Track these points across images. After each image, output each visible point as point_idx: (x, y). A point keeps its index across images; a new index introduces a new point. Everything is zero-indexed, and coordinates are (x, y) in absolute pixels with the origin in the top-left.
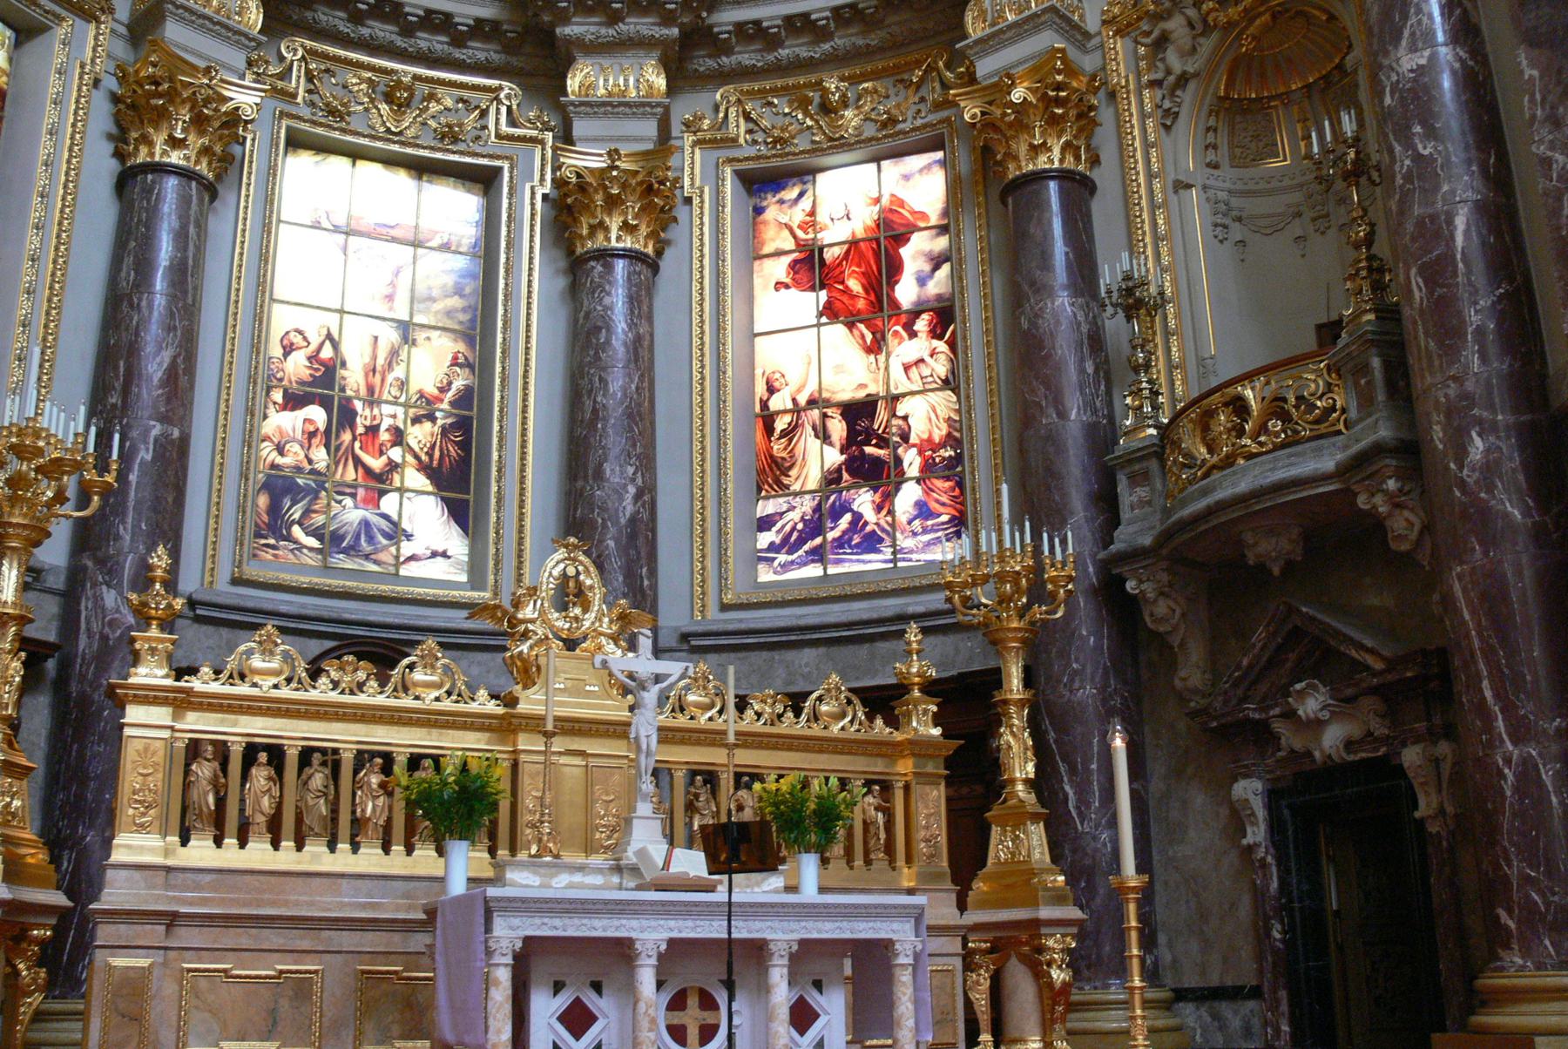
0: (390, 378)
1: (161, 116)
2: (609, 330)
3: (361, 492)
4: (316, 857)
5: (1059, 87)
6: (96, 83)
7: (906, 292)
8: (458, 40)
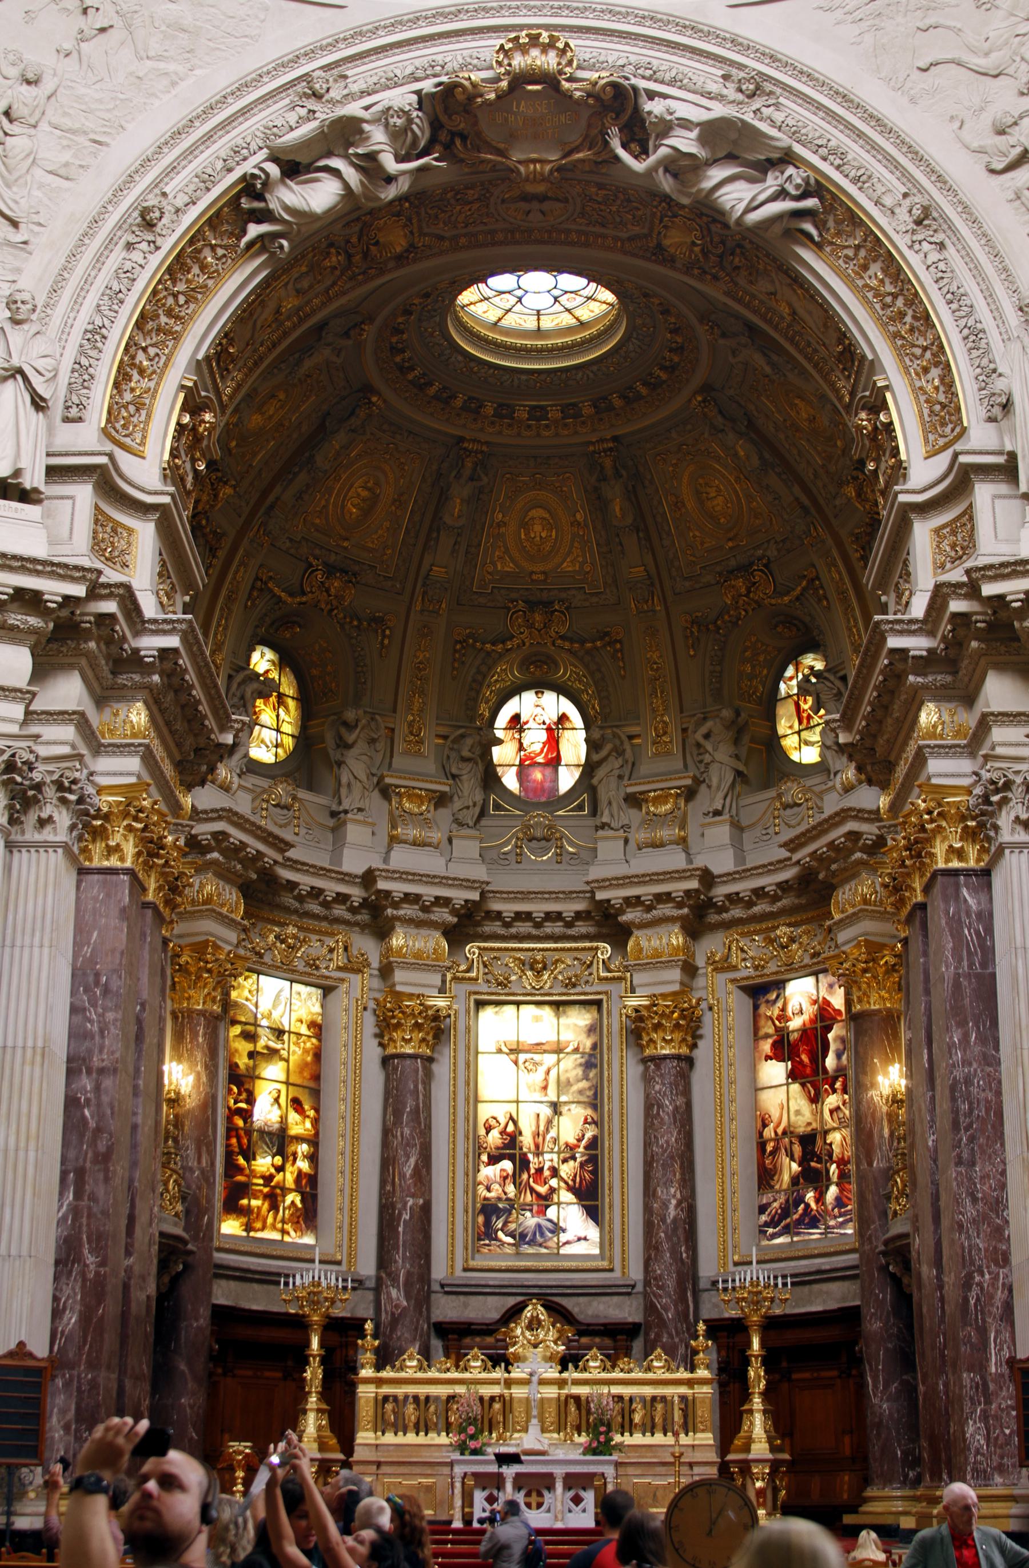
0: (548, 1137)
1: (398, 1026)
2: (660, 1106)
3: (535, 1208)
4: (432, 1439)
5: (866, 962)
6: (365, 1009)
7: (830, 1062)
8: (569, 925)
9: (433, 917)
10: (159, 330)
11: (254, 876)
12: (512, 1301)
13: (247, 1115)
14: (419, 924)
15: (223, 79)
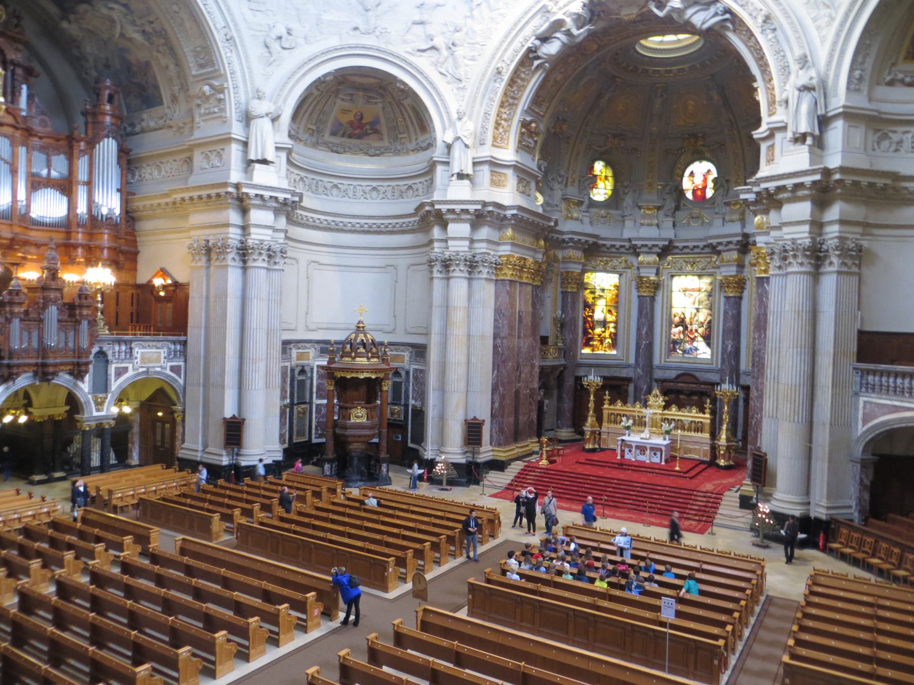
2: (728, 313)
8: (703, 249)
9: (653, 251)
10: (510, 105)
11: (587, 247)
12: (680, 372)
13: (592, 317)
14: (648, 253)
15: (518, 11)
